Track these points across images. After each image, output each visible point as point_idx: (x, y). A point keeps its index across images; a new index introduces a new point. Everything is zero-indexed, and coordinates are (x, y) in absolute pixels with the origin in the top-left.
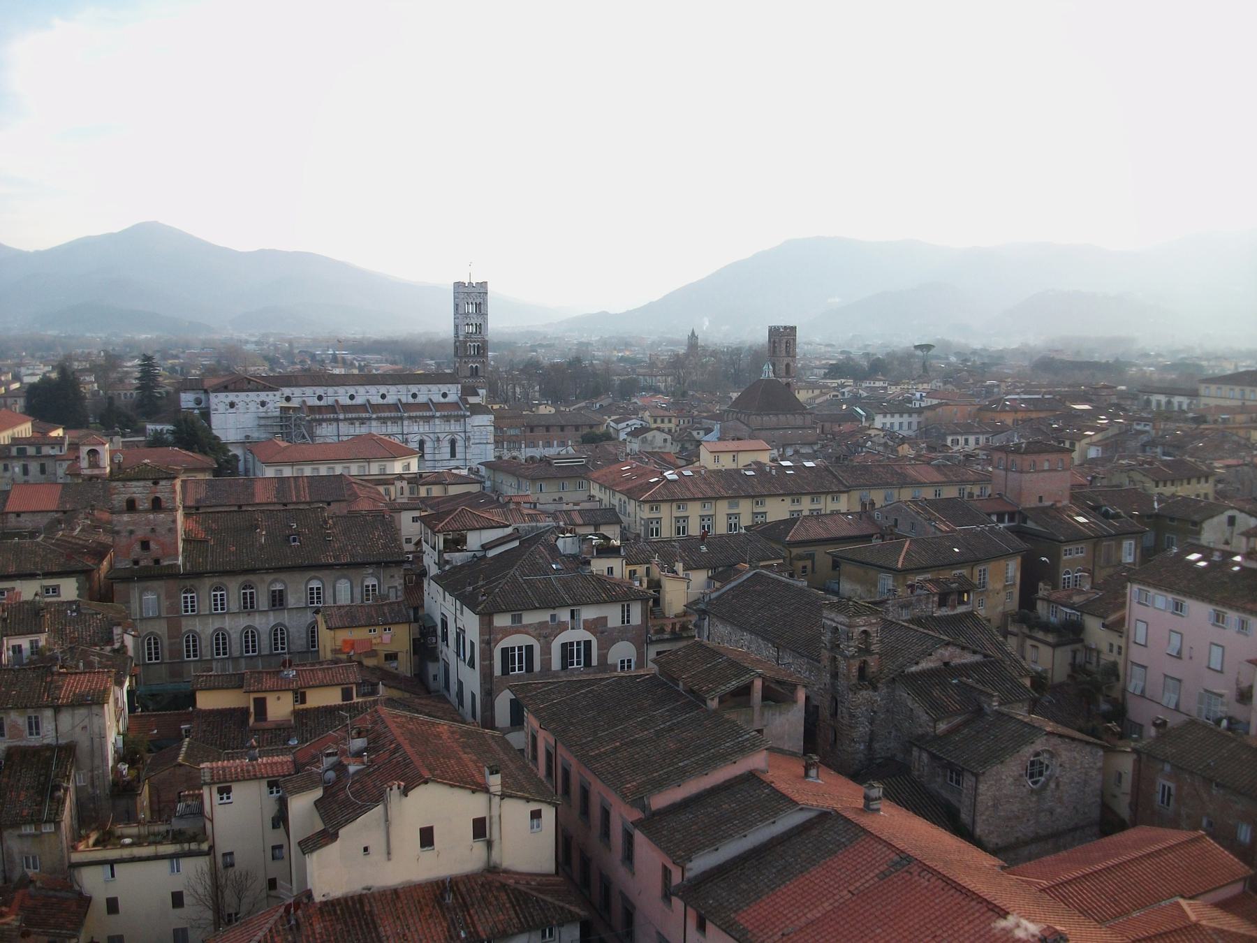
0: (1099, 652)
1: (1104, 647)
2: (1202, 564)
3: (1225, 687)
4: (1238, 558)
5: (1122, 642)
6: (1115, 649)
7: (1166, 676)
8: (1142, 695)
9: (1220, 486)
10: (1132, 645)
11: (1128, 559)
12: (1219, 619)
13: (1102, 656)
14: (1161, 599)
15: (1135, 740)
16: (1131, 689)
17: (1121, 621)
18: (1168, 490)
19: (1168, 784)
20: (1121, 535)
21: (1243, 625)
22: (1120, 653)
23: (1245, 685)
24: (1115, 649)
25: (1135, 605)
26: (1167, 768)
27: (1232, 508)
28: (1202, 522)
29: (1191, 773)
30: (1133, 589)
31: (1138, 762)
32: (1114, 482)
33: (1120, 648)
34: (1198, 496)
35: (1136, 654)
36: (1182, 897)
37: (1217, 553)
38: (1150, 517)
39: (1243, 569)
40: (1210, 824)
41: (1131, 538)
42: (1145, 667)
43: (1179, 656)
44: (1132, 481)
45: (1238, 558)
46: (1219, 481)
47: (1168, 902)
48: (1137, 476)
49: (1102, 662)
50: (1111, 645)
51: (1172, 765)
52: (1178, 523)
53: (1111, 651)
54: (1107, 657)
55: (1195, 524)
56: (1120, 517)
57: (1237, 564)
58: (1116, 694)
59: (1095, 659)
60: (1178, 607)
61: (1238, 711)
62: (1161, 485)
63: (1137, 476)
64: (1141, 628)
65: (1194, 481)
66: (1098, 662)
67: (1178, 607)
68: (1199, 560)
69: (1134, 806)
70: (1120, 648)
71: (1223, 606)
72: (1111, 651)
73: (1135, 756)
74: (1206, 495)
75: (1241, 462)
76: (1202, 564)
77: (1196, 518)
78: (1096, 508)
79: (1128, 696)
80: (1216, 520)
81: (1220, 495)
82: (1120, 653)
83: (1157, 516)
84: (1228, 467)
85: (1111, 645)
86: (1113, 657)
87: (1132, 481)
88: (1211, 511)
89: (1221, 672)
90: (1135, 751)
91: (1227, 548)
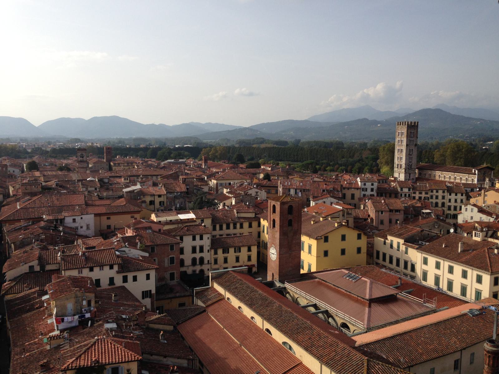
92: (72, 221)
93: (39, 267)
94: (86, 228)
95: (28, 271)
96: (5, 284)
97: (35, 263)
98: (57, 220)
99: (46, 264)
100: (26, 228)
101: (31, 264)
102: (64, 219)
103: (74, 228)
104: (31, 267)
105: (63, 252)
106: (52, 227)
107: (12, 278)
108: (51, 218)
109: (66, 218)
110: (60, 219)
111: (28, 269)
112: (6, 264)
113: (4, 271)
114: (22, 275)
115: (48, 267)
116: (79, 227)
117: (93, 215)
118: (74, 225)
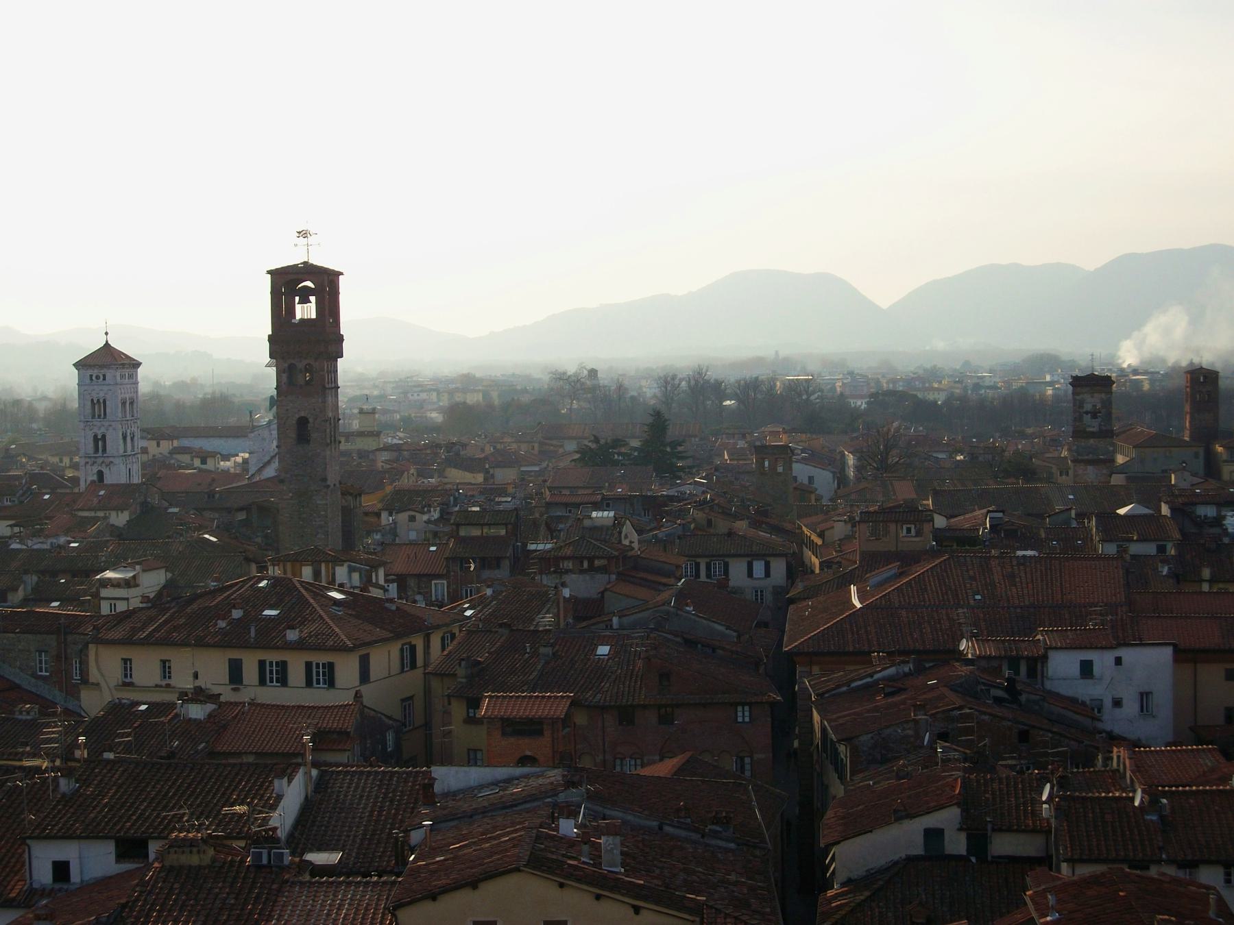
92: (1075, 670)
93: (963, 837)
94: (1137, 707)
95: (920, 851)
96: (830, 893)
97: (947, 818)
98: (1014, 662)
99: (994, 830)
100: (894, 687)
101: (931, 821)
102: (1045, 658)
103: (1083, 703)
104: (933, 836)
105: (1063, 783)
106: (997, 687)
107: (858, 872)
108: (991, 650)
109: (1051, 654)
110: (1028, 658)
111: (920, 839)
112: (830, 813)
114: (896, 863)
115: (1003, 845)
116: (1108, 703)
117: (1168, 652)
118: (1086, 691)
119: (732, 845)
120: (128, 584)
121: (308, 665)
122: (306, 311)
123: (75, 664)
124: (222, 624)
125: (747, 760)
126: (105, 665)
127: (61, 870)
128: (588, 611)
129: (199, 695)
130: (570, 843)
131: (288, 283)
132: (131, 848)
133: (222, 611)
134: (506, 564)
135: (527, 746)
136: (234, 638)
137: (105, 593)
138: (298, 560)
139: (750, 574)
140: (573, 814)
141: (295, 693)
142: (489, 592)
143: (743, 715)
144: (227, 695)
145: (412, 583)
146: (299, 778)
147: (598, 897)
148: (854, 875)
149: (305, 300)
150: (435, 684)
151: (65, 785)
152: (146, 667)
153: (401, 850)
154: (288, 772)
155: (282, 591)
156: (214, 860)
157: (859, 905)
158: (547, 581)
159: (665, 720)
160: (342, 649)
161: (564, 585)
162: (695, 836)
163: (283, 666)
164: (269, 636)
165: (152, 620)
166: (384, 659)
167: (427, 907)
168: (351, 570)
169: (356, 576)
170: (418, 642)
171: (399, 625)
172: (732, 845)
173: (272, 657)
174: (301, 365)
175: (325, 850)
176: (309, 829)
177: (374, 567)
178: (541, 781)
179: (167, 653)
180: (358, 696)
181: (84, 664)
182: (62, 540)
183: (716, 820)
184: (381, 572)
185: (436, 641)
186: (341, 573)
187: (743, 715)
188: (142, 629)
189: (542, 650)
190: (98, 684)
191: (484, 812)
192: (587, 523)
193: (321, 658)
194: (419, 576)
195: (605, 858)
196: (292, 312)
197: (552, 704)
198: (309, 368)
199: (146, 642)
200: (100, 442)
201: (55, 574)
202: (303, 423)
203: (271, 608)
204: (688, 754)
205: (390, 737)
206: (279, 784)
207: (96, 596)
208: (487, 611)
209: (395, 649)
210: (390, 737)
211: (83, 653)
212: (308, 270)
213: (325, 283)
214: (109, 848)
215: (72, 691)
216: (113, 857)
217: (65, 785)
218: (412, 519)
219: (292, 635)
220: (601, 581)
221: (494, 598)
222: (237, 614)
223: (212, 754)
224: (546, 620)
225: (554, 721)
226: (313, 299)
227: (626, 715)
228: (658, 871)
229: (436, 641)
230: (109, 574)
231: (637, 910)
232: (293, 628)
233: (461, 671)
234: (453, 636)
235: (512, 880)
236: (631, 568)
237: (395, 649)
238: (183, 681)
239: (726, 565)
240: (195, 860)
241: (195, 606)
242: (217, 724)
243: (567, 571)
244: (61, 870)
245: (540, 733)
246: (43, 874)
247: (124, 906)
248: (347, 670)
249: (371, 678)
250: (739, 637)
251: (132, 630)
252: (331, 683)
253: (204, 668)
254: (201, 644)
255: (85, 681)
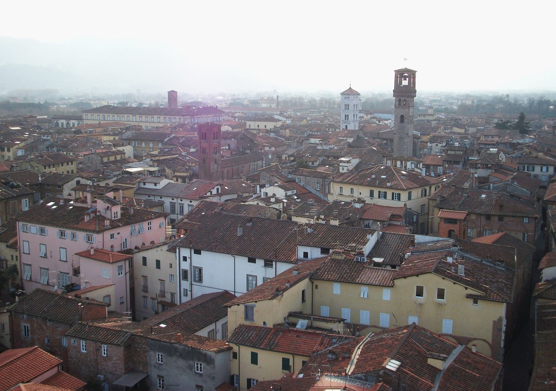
0: (7, 261)
1: (9, 258)
2: (54, 207)
3: (67, 268)
4: (72, 202)
5: (17, 254)
6: (14, 258)
7: (41, 268)
8: (31, 279)
9: (81, 166)
10: (23, 255)
11: (27, 209)
12: (62, 234)
13: (8, 263)
14: (34, 228)
15: (8, 305)
16: (25, 278)
17: (16, 243)
18: (47, 170)
19: (26, 325)
20: (20, 197)
21: (74, 236)
22: (17, 260)
23: (76, 266)
24: (14, 258)
25: (21, 233)
26: (25, 316)
27: (78, 177)
28: (63, 185)
29: (36, 317)
30: (20, 225)
31: (11, 316)
32: (23, 168)
33: (17, 257)
34: (68, 172)
35: (25, 259)
36: (23, 382)
37: (62, 201)
38: (37, 185)
39: (74, 207)
40: (49, 340)
41: (26, 197)
42: (30, 265)
43: (46, 256)
44: (32, 166)
45: (72, 202)
46: (80, 163)
47: (14, 387)
48: (34, 164)
49: (9, 266)
50: (12, 256)
51: (27, 315)
52: (50, 187)
53: (13, 259)
54: (11, 263)
55: (59, 186)
56: (20, 187)
57: (72, 205)
58: (18, 282)
59: (5, 266)
60: (42, 231)
61: (75, 280)
62: (47, 167)
63: (34, 164)
64: (26, 244)
65: (65, 164)
66: (7, 266)
67: (42, 231)
68: (53, 205)
69: (12, 340)
70: (17, 257)
71: (64, 228)
72: (13, 259)
73: (9, 314)
74: (72, 171)
75: (90, 153)
76: (54, 207)
77: (60, 183)
78: (7, 183)
79: (24, 282)
80: (70, 183)
81: (80, 170)
82: (17, 260)
83: (41, 185)
84: (85, 155)
85: (12, 256)
86: (13, 263)
87: (32, 166)
88: (67, 178)
89: (66, 261)
90: (8, 311)
91: (70, 198)
96: (540, 283)
107: (550, 278)
112: (544, 258)
113: (540, 267)
119: (504, 269)
120: (348, 162)
121: (393, 193)
122: (405, 83)
123: (327, 188)
124: (369, 179)
125: (526, 234)
126: (335, 188)
127: (306, 255)
128: (483, 181)
129: (360, 201)
130: (450, 265)
131: (401, 74)
132: (325, 251)
133: (369, 175)
134: (461, 163)
135: (452, 227)
136: (372, 184)
137: (341, 164)
138: (396, 160)
139: (541, 170)
140: (451, 256)
141: (389, 202)
142: (452, 174)
143: (526, 220)
144: (368, 201)
145: (432, 167)
146: (375, 234)
147: (454, 283)
148: (549, 279)
149: (405, 79)
150: (431, 202)
151: (309, 230)
152: (347, 189)
153: (402, 259)
154: (372, 232)
155: (387, 170)
156: (345, 258)
157: (548, 289)
158: (472, 171)
159: (501, 218)
160: (403, 190)
161: (476, 173)
162: (492, 265)
163: (385, 193)
164: (382, 184)
165: (349, 176)
166: (416, 193)
167: (403, 280)
168: (412, 163)
169: (413, 165)
170: (428, 188)
171: (420, 182)
172: (504, 269)
173: (383, 190)
174: (402, 99)
175: (378, 257)
176: (375, 252)
177: (419, 163)
178: (447, 243)
179: (353, 187)
180: (405, 205)
181: (329, 188)
182: (332, 146)
183: (499, 261)
184: (421, 164)
185: (433, 188)
186: (409, 164)
187: (526, 220)
188: (346, 179)
189: (464, 195)
190: (333, 194)
191: (428, 251)
192: (488, 152)
193: (397, 192)
194: (434, 165)
195: (459, 271)
196: (401, 83)
197: (460, 215)
198: (405, 100)
199: (347, 183)
200: (347, 117)
201: (329, 157)
202: (402, 117)
203: (384, 175)
204: (504, 232)
205: (415, 218)
206: (369, 236)
207: (339, 165)
208: (451, 180)
209: (420, 190)
210: (415, 218)
211: (329, 184)
212: (407, 70)
213: (411, 74)
214: (319, 250)
215: (326, 195)
216: (320, 252)
217: (309, 230)
218: (437, 145)
219: (389, 184)
220: (489, 171)
221: (453, 175)
222: (373, 176)
223: (361, 219)
224: (466, 185)
225: (460, 220)
226: (407, 79)
227: (488, 217)
228: (476, 276)
229: (433, 188)
230: (342, 159)
231: (466, 288)
232: (389, 182)
233: (438, 199)
234: (439, 187)
235: (430, 274)
236: (499, 168)
237: (420, 190)
238: (356, 195)
239: (534, 167)
240: (340, 258)
241: (362, 173)
242: (363, 210)
243: (479, 168)
244: (306, 255)
245: (456, 223)
246: (301, 255)
247: (318, 269)
248: (404, 196)
249: (411, 200)
250: (531, 193)
251: (344, 179)
252: (399, 199)
253: (363, 192)
254: (361, 184)
255: (329, 192)
